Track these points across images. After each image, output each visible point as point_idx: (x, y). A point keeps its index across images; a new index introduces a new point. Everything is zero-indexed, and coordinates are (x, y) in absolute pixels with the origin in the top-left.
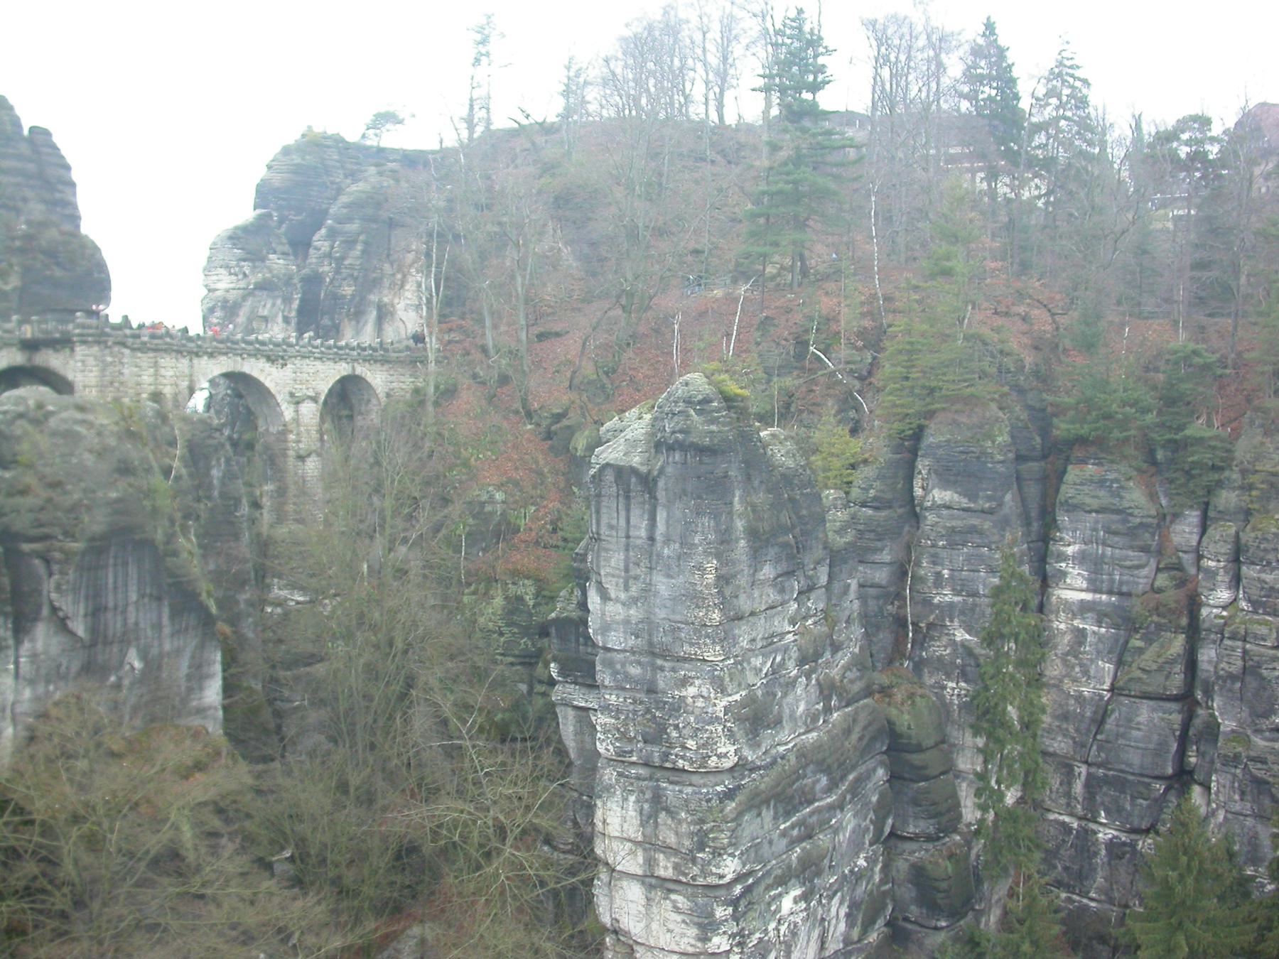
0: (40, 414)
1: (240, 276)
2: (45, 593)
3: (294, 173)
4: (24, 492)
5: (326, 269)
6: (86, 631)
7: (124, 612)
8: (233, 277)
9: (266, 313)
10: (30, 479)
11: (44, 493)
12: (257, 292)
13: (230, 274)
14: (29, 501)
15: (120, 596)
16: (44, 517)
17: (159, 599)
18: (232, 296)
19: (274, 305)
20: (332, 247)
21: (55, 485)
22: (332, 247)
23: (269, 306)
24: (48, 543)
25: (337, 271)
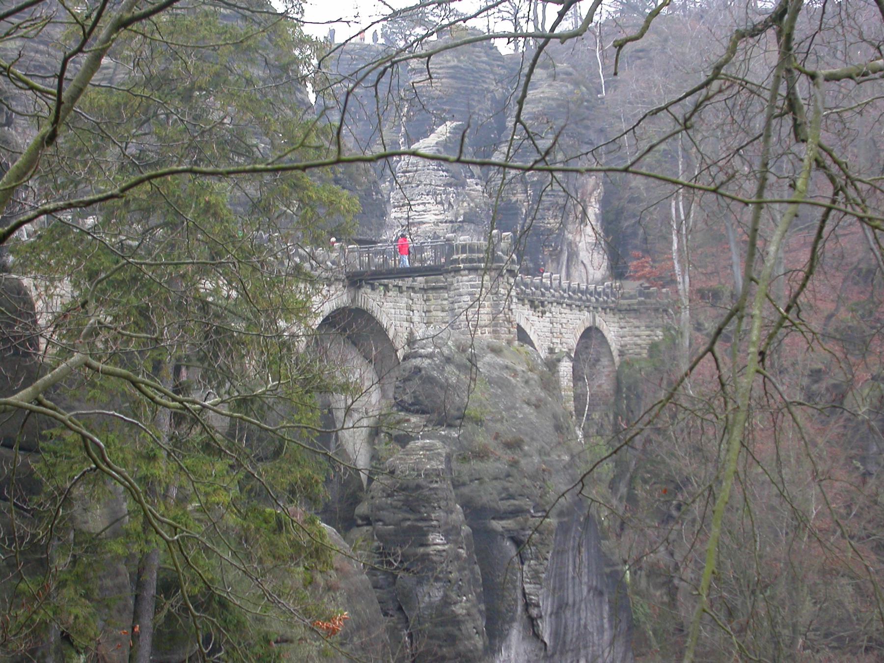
0: (463, 359)
1: (446, 206)
2: (518, 583)
3: (452, 77)
4: (482, 455)
5: (521, 197)
6: (551, 634)
7: (579, 610)
10: (482, 438)
11: (507, 456)
12: (466, 226)
14: (490, 467)
15: (576, 589)
16: (513, 487)
17: (601, 594)
21: (514, 445)
24: (520, 519)
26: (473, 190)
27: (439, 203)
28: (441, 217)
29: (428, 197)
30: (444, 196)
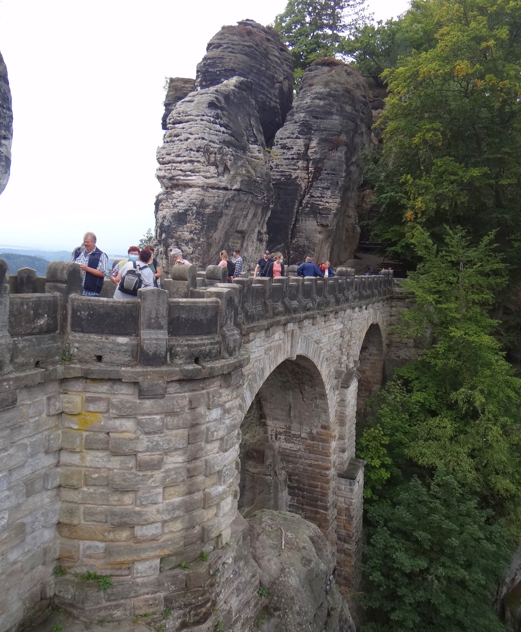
1: (221, 169)
8: (212, 169)
9: (245, 228)
13: (210, 164)
18: (213, 198)
19: (255, 215)
20: (307, 147)
22: (307, 147)
23: (250, 216)
25: (316, 176)
26: (255, 158)
27: (213, 164)
28: (212, 181)
29: (198, 154)
30: (219, 157)
